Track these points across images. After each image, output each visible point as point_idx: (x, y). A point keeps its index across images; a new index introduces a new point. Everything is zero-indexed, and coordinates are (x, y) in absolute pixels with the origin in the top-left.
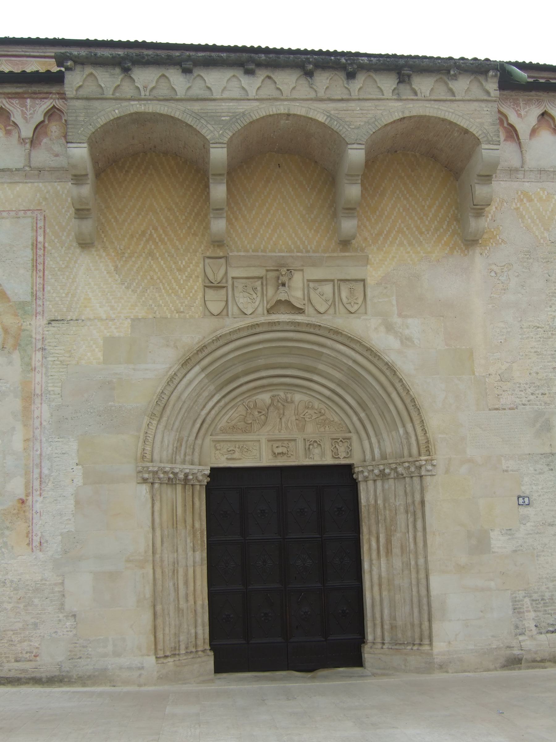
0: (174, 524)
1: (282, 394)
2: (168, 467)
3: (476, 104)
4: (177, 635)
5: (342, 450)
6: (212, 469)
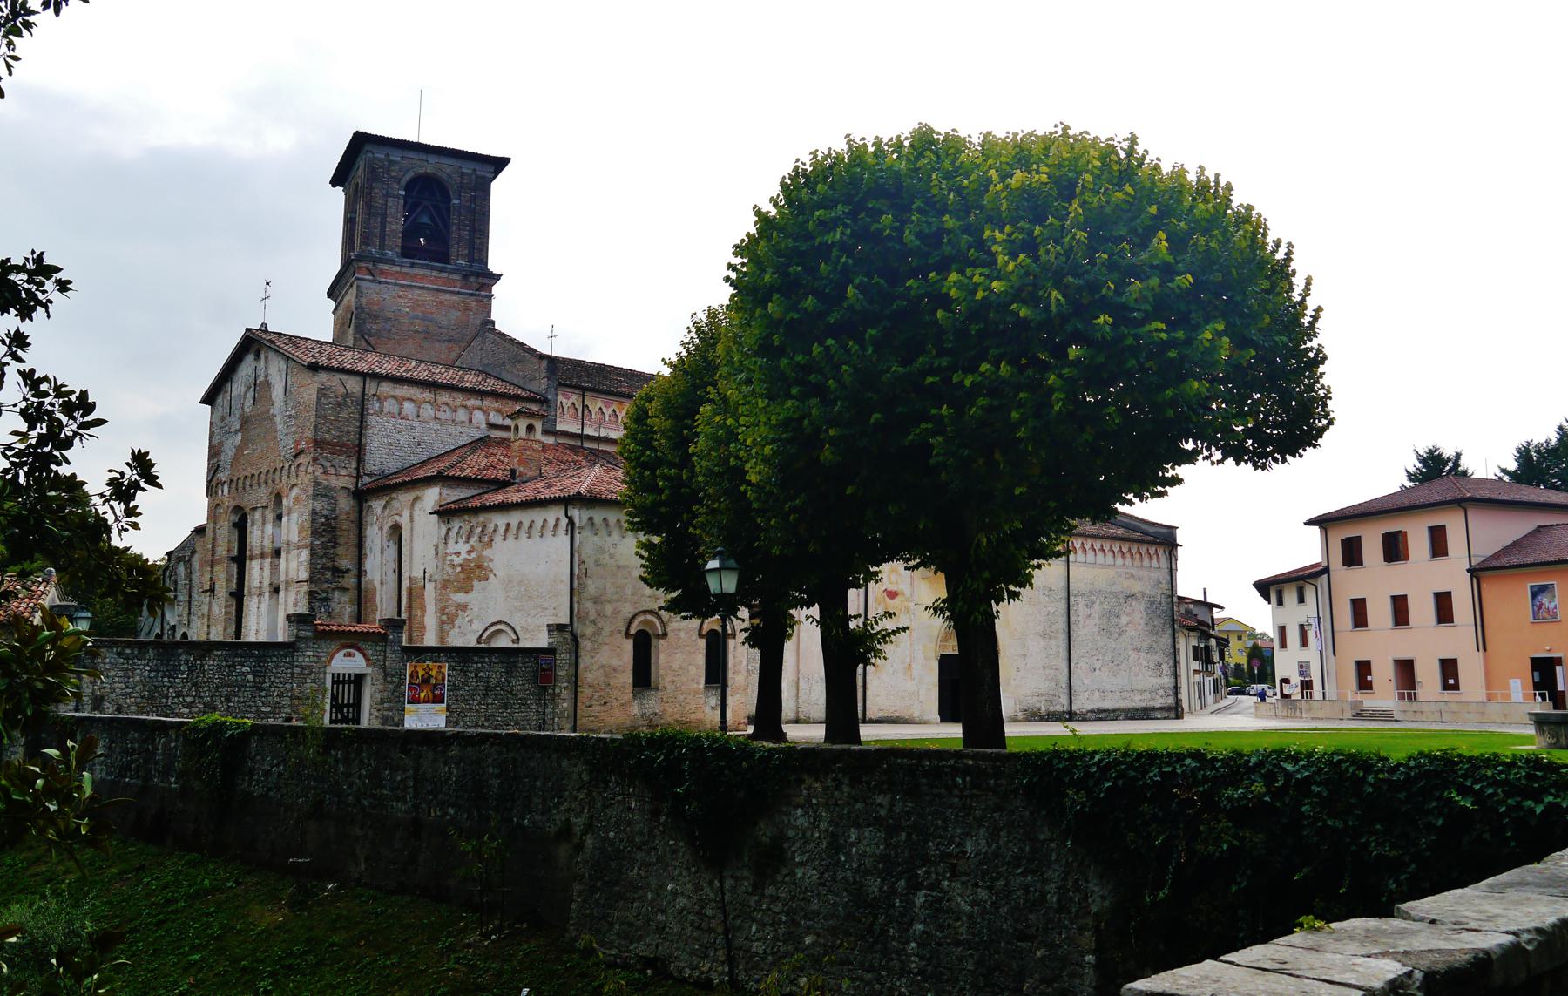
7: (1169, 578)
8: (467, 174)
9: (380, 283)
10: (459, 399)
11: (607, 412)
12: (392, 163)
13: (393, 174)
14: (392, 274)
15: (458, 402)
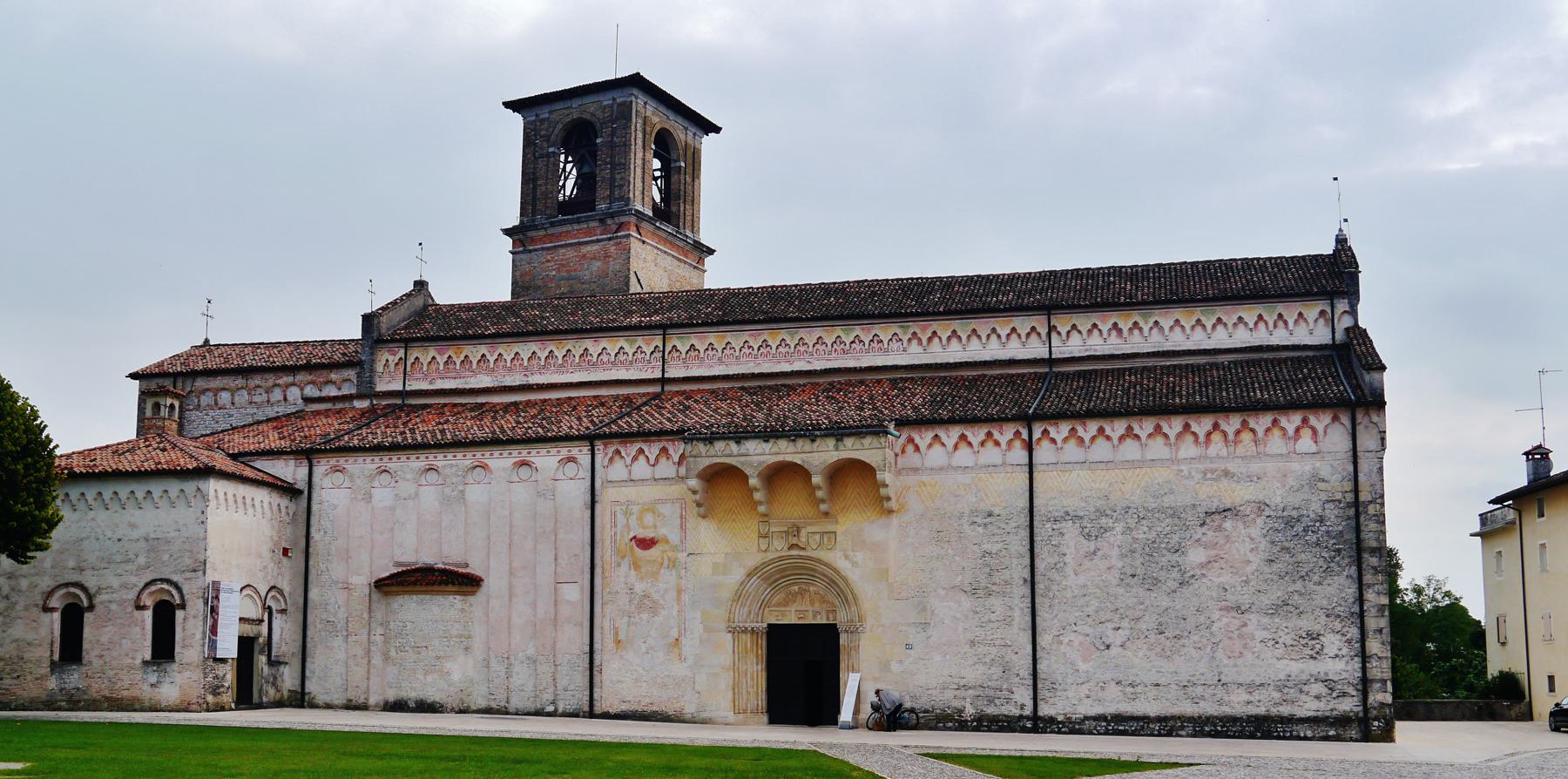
0: (746, 653)
1: (804, 587)
2: (741, 625)
3: (874, 451)
7: (1351, 468)
9: (530, 251)
10: (271, 379)
11: (441, 360)
12: (542, 121)
13: (543, 133)
14: (542, 240)
15: (270, 383)
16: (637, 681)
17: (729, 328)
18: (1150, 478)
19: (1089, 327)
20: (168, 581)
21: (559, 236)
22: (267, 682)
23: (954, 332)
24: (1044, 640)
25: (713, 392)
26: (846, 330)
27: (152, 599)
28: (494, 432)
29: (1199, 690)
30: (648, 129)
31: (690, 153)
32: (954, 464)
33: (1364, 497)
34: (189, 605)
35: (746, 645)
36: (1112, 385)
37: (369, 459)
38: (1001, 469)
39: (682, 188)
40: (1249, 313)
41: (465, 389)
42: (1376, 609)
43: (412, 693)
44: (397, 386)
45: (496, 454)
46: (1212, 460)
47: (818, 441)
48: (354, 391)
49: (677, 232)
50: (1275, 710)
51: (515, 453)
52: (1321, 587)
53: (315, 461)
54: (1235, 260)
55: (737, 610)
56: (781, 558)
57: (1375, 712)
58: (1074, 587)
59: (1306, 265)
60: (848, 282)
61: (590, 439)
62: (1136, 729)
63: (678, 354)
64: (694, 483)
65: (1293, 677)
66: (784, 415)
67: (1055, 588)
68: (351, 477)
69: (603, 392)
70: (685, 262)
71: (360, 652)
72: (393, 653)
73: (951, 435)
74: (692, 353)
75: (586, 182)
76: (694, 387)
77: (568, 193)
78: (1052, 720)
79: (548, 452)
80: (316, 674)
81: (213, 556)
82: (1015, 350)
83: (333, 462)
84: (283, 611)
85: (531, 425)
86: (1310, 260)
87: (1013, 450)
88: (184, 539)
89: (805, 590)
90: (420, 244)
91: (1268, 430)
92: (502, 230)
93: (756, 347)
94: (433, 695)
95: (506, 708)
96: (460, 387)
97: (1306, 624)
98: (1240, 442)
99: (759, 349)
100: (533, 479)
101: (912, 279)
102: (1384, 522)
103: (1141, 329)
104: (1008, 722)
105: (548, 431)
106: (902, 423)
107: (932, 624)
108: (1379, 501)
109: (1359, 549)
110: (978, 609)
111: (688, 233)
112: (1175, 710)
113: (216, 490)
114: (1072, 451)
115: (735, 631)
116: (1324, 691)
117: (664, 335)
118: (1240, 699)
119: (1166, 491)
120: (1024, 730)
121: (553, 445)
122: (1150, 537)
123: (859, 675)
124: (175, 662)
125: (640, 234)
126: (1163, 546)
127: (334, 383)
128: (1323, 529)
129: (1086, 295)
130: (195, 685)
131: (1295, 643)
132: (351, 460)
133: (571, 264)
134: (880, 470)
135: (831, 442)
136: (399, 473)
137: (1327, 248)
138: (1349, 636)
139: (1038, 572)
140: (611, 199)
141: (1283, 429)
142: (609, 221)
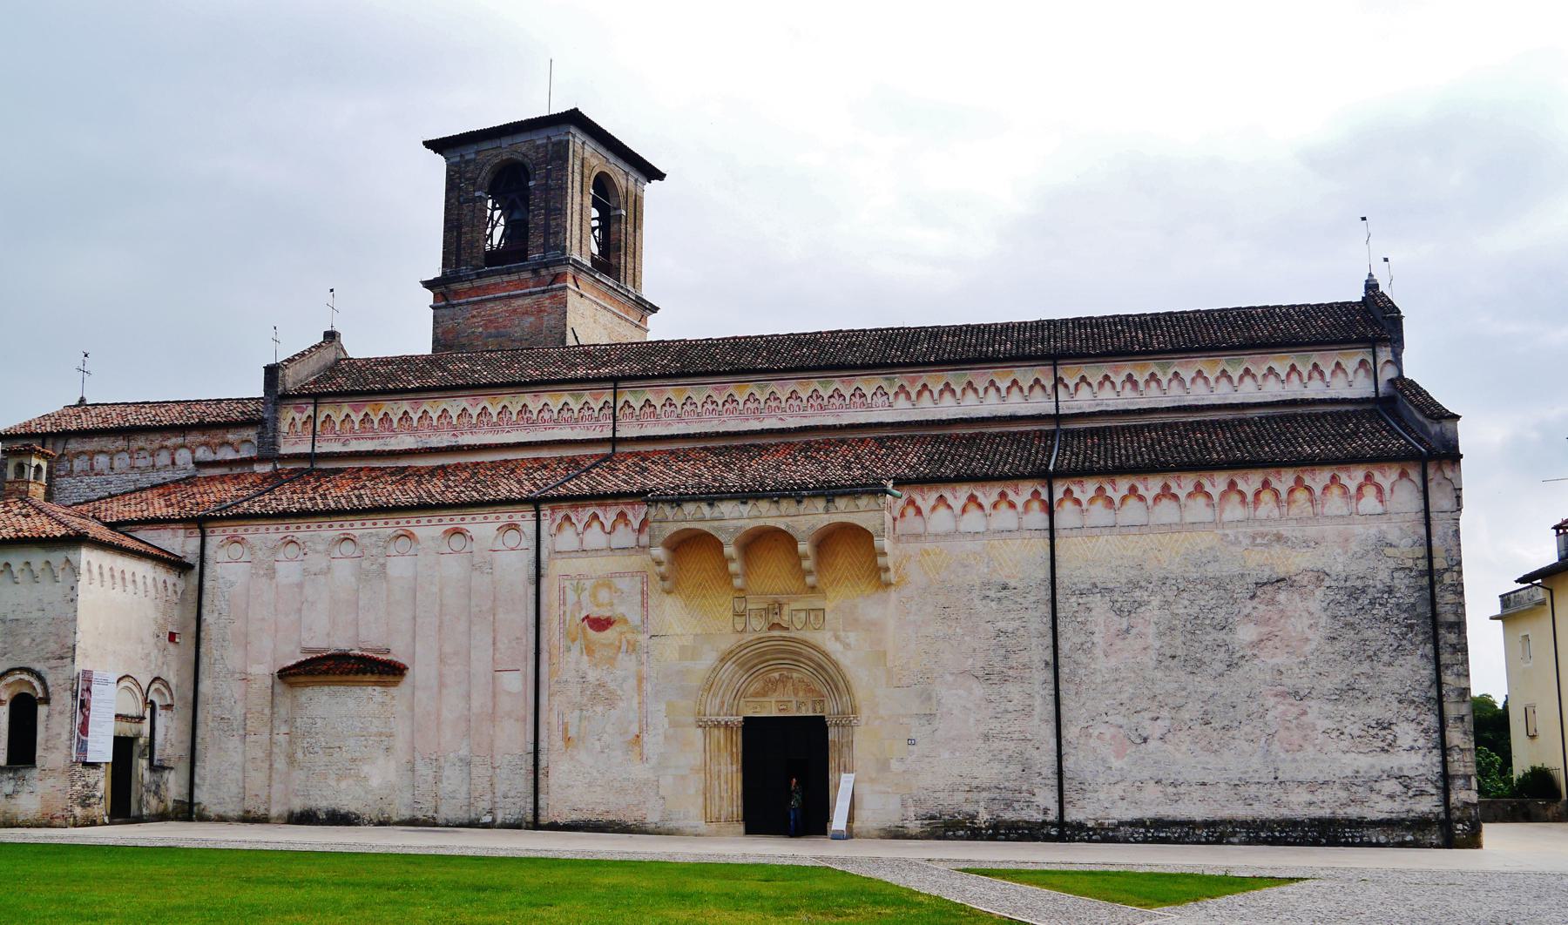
0: (719, 750)
2: (713, 718)
4: (719, 811)
5: (818, 708)
6: (744, 718)
7: (1423, 531)
8: (542, 145)
9: (453, 306)
10: (157, 440)
11: (357, 418)
12: (468, 162)
14: (467, 293)
15: (156, 445)
16: (590, 785)
17: (690, 381)
18: (1191, 544)
19: (1101, 379)
20: (29, 671)
21: (486, 289)
22: (148, 791)
23: (947, 385)
24: (1069, 733)
25: (672, 453)
26: (823, 382)
27: (8, 692)
28: (420, 497)
29: (1253, 789)
30: (586, 172)
31: (631, 200)
32: (962, 528)
33: (1439, 563)
34: (54, 698)
35: (719, 742)
36: (1132, 442)
37: (272, 528)
38: (1017, 534)
39: (623, 238)
40: (1281, 363)
41: (384, 451)
42: (1456, 693)
43: (322, 802)
44: (305, 448)
45: (424, 521)
46: (1261, 522)
47: (806, 502)
48: (253, 454)
49: (618, 286)
50: (1341, 812)
51: (446, 520)
52: (1391, 669)
53: (208, 531)
54: (1254, 308)
55: (709, 701)
56: (760, 640)
57: (1458, 813)
58: (1104, 670)
59: (1336, 313)
60: (820, 333)
61: (535, 503)
62: (1180, 836)
63: (631, 410)
64: (659, 552)
65: (1362, 773)
66: (761, 476)
67: (1082, 672)
68: (252, 548)
69: (544, 454)
70: (627, 320)
71: (261, 755)
72: (300, 755)
73: (958, 496)
74: (648, 410)
75: (516, 231)
76: (650, 448)
77: (496, 242)
78: (1080, 826)
79: (486, 518)
80: (207, 782)
81: (85, 638)
82: (1016, 405)
83: (230, 531)
84: (168, 707)
85: (462, 489)
86: (1338, 308)
87: (1031, 513)
88: (49, 621)
89: (787, 677)
90: (332, 290)
91: (1326, 488)
92: (422, 282)
93: (720, 403)
94: (347, 804)
95: (434, 819)
96: (378, 448)
97: (1375, 711)
98: (1294, 501)
99: (724, 405)
100: (467, 549)
101: (892, 329)
102: (1462, 594)
103: (1158, 382)
104: (1029, 829)
105: (485, 494)
106: (900, 482)
107: (939, 715)
108: (1456, 568)
109: (1434, 622)
110: (992, 698)
111: (630, 287)
112: (1225, 814)
113: (89, 563)
114: (1099, 514)
115: (703, 725)
116: (1399, 789)
117: (615, 388)
118: (1300, 799)
119: (1210, 558)
120: (1048, 838)
121: (492, 510)
122: (1191, 612)
123: (853, 775)
124: (35, 767)
125: (578, 287)
126: (1208, 622)
127: (231, 445)
128: (1393, 601)
129: (1094, 344)
130: (59, 795)
131: (1364, 733)
132: (252, 529)
133: (500, 320)
134: (878, 536)
135: (820, 504)
136: (309, 544)
137: (1356, 295)
138: (1426, 725)
139: (1061, 654)
140: (546, 247)
141: (1343, 487)
142: (543, 272)
